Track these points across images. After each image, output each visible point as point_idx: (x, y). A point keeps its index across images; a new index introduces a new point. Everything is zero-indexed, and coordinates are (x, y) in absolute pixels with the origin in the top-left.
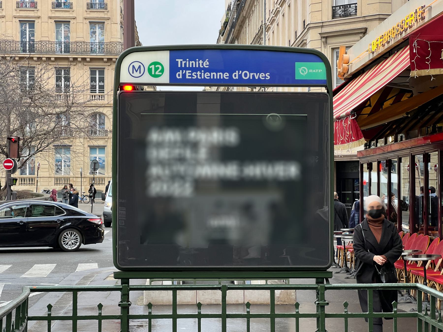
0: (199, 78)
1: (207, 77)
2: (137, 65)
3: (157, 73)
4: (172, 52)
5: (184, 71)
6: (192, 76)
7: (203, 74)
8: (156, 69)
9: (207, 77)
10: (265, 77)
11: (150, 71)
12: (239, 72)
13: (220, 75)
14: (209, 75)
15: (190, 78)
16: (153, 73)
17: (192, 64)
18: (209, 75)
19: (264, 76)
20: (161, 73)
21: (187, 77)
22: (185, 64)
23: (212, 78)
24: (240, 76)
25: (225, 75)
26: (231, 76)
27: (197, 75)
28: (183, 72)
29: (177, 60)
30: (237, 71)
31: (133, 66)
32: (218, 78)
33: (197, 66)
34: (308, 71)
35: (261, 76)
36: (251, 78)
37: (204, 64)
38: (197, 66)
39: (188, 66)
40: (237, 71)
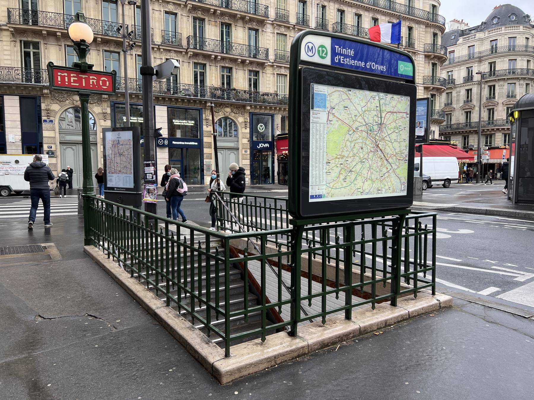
2: (310, 45)
3: (323, 55)
4: (335, 39)
8: (323, 51)
11: (319, 51)
26: (365, 65)
31: (308, 47)
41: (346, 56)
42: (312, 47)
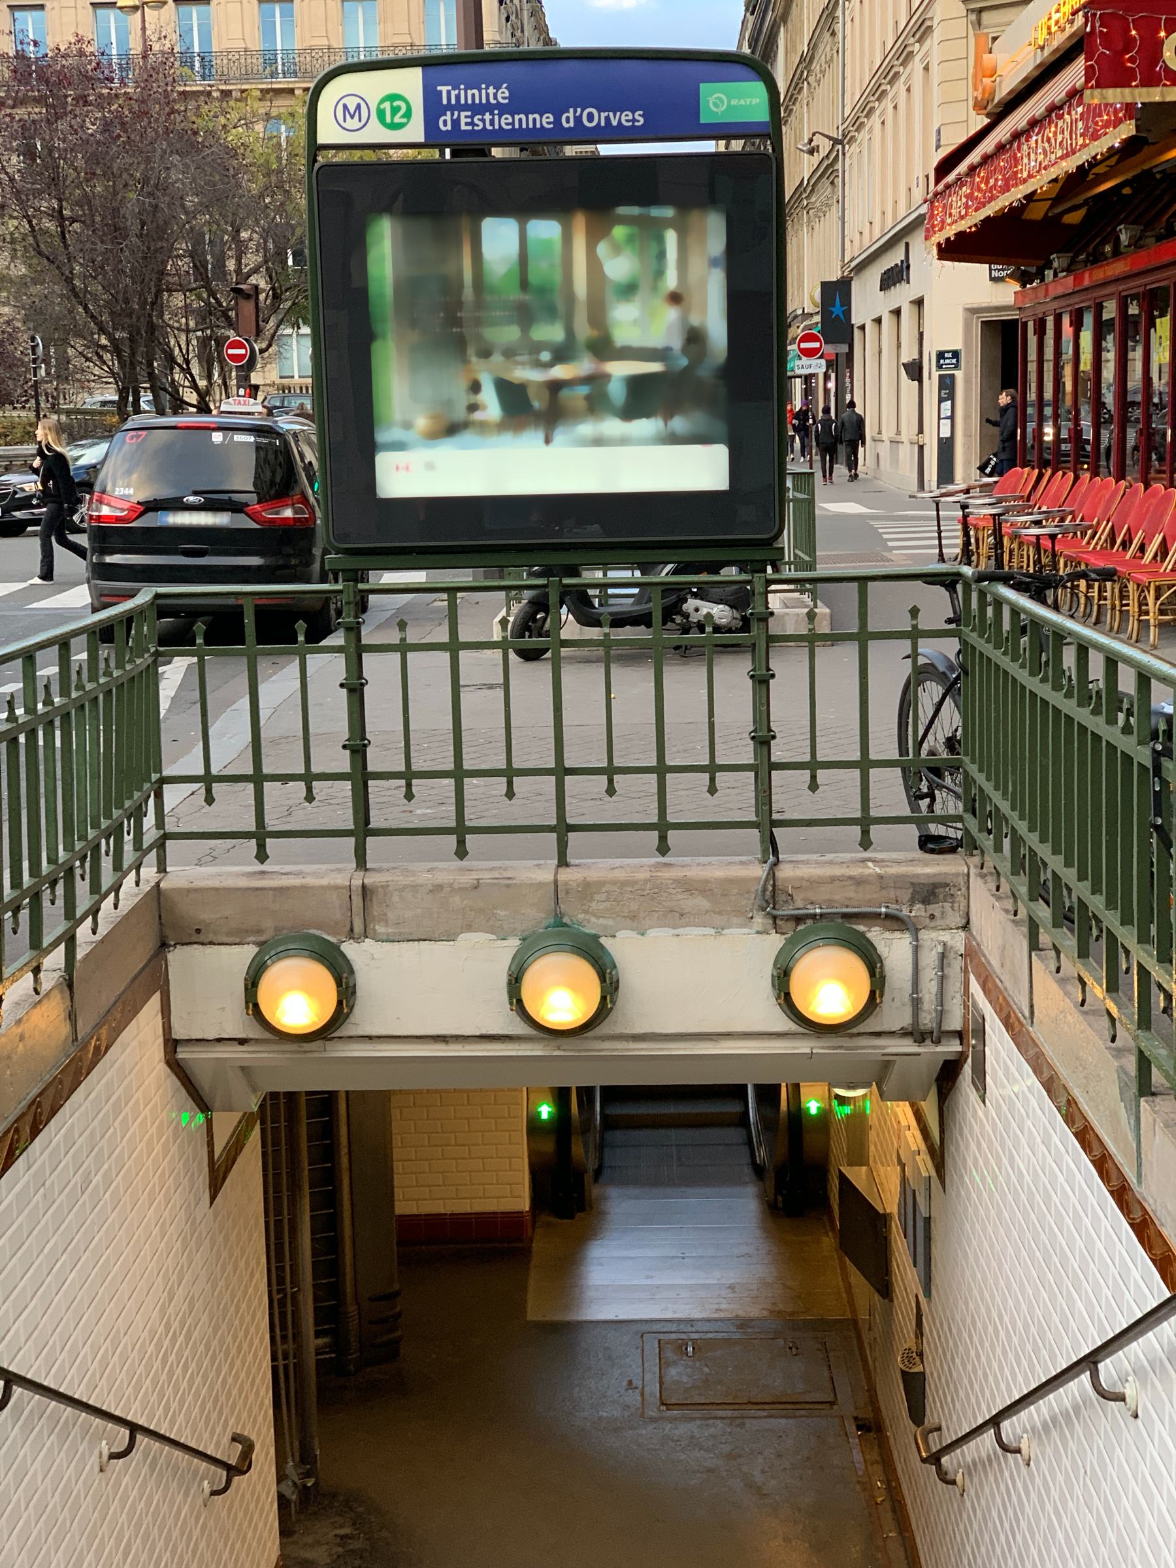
0: (489, 127)
1: (507, 124)
2: (352, 104)
3: (397, 120)
5: (456, 113)
6: (473, 124)
7: (496, 117)
8: (395, 111)
9: (507, 124)
10: (634, 120)
11: (381, 114)
12: (575, 112)
13: (534, 120)
14: (510, 120)
15: (470, 128)
16: (388, 120)
17: (473, 95)
18: (510, 120)
19: (631, 117)
20: (405, 120)
21: (463, 127)
22: (458, 97)
23: (517, 126)
24: (578, 120)
25: (544, 120)
27: (483, 121)
28: (452, 115)
29: (439, 88)
30: (571, 110)
31: (345, 107)
32: (531, 126)
33: (484, 101)
34: (729, 102)
35: (623, 119)
36: (603, 124)
37: (499, 95)
38: (484, 101)
39: (463, 102)
40: (571, 110)
41: (477, 109)
42: (358, 107)
